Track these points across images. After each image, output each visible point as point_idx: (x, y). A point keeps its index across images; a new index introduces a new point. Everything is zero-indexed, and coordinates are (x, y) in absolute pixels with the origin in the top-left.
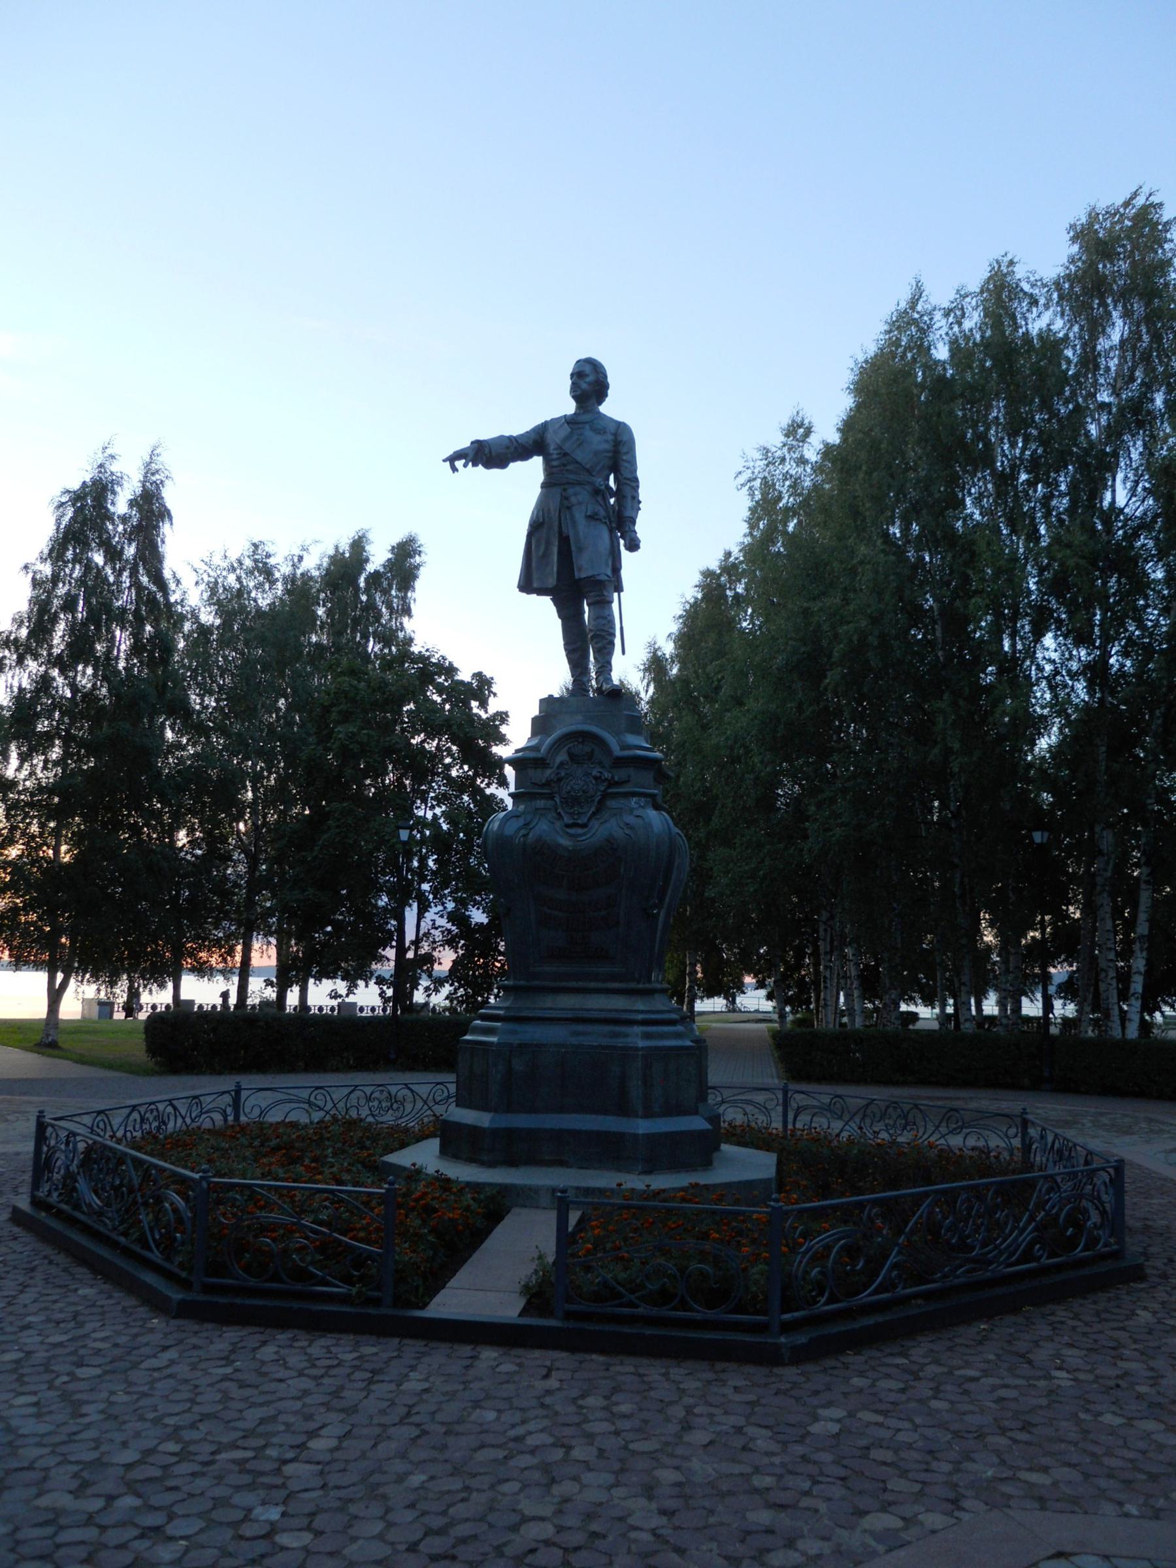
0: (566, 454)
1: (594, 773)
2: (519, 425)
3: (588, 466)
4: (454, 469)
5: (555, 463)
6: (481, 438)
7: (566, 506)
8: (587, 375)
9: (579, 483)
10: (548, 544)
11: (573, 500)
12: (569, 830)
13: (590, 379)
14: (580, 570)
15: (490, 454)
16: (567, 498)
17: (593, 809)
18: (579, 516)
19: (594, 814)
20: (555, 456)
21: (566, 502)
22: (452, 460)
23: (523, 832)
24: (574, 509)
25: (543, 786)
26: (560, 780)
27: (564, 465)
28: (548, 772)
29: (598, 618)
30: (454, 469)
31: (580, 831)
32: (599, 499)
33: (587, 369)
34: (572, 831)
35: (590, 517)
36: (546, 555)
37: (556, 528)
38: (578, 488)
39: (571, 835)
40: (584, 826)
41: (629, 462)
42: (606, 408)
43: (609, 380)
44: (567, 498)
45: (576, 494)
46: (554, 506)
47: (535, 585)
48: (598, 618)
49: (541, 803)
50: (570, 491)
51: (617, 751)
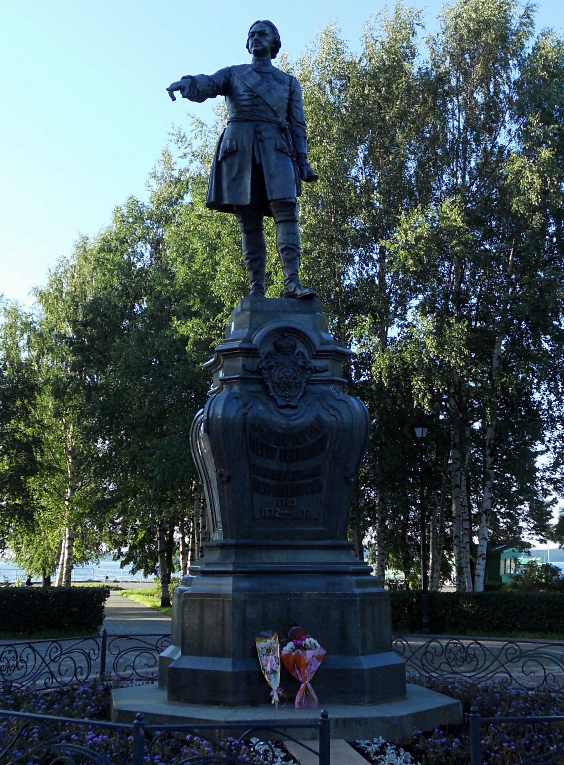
0: (258, 96)
1: (300, 363)
2: (210, 69)
3: (275, 108)
4: (174, 99)
5: (245, 103)
6: (193, 74)
7: (258, 140)
8: (267, 35)
9: (269, 122)
10: (241, 170)
11: (265, 134)
12: (281, 411)
13: (269, 38)
14: (271, 192)
15: (195, 89)
16: (259, 133)
17: (301, 393)
18: (269, 146)
19: (302, 397)
20: (245, 97)
21: (258, 136)
22: (171, 90)
23: (243, 411)
24: (266, 141)
25: (255, 371)
26: (271, 368)
27: (256, 105)
28: (258, 360)
29: (288, 234)
30: (174, 99)
31: (292, 412)
32: (283, 135)
33: (268, 30)
34: (286, 411)
35: (278, 149)
36: (237, 179)
37: (249, 157)
38: (268, 126)
39: (283, 415)
40: (295, 407)
41: (300, 109)
42: (275, 63)
43: (281, 40)
44: (259, 133)
45: (267, 130)
46: (247, 138)
47: (226, 202)
48: (288, 234)
49: (253, 388)
50: (262, 127)
51: (319, 348)
